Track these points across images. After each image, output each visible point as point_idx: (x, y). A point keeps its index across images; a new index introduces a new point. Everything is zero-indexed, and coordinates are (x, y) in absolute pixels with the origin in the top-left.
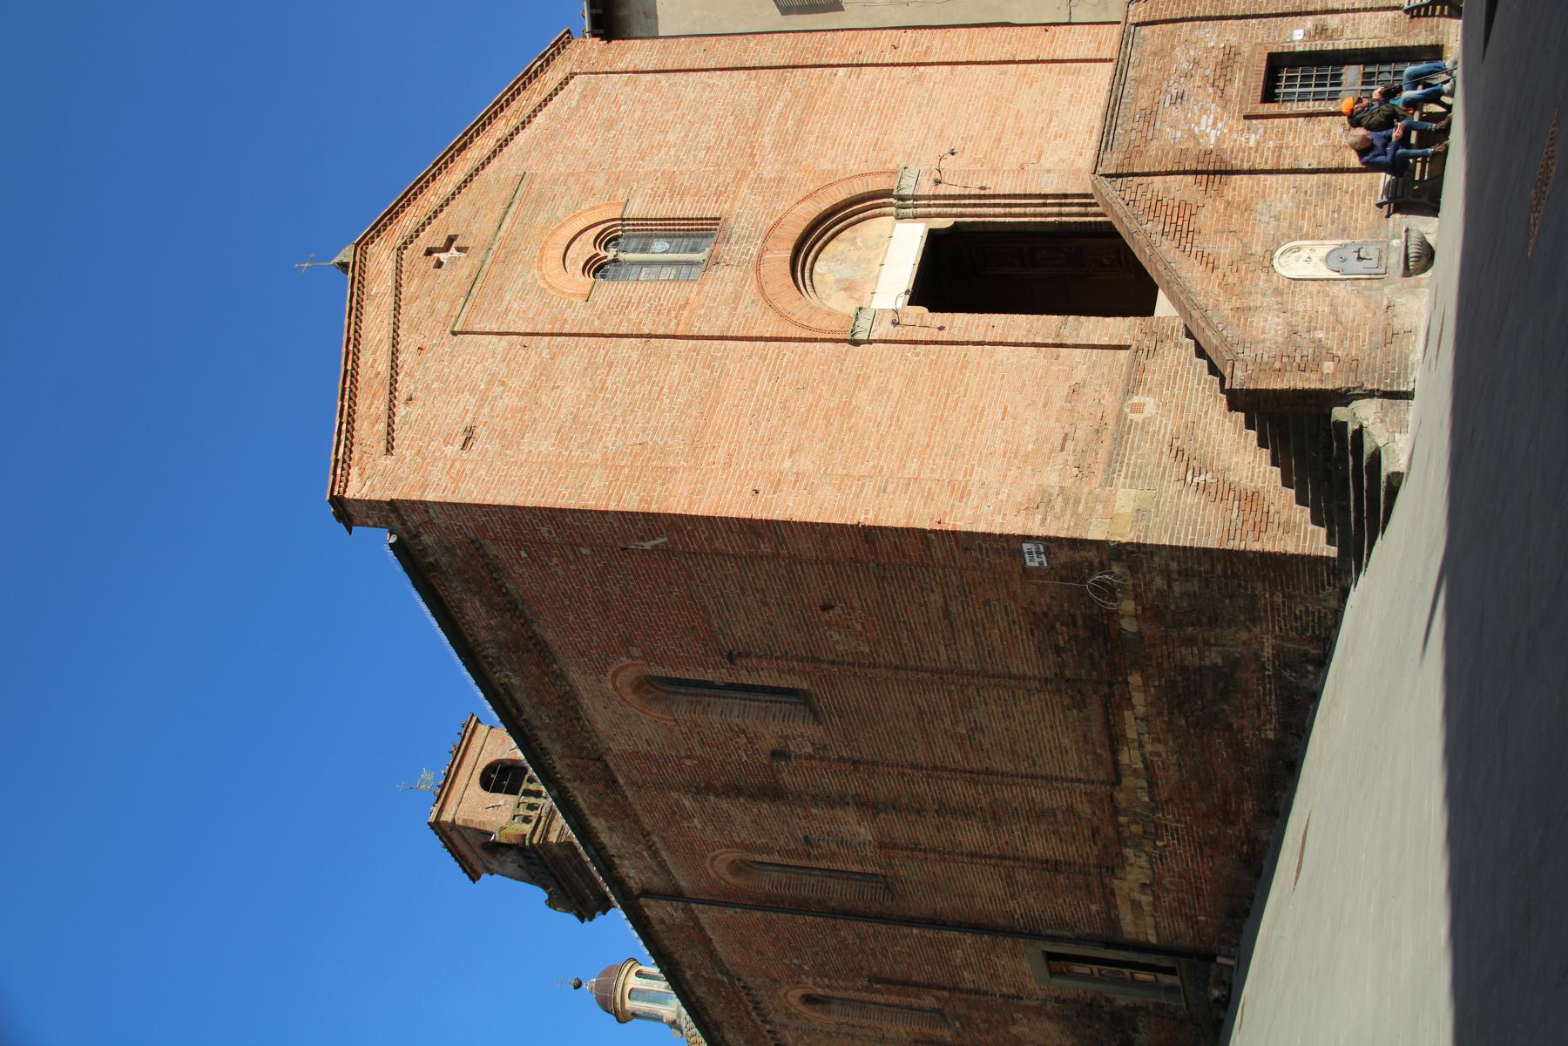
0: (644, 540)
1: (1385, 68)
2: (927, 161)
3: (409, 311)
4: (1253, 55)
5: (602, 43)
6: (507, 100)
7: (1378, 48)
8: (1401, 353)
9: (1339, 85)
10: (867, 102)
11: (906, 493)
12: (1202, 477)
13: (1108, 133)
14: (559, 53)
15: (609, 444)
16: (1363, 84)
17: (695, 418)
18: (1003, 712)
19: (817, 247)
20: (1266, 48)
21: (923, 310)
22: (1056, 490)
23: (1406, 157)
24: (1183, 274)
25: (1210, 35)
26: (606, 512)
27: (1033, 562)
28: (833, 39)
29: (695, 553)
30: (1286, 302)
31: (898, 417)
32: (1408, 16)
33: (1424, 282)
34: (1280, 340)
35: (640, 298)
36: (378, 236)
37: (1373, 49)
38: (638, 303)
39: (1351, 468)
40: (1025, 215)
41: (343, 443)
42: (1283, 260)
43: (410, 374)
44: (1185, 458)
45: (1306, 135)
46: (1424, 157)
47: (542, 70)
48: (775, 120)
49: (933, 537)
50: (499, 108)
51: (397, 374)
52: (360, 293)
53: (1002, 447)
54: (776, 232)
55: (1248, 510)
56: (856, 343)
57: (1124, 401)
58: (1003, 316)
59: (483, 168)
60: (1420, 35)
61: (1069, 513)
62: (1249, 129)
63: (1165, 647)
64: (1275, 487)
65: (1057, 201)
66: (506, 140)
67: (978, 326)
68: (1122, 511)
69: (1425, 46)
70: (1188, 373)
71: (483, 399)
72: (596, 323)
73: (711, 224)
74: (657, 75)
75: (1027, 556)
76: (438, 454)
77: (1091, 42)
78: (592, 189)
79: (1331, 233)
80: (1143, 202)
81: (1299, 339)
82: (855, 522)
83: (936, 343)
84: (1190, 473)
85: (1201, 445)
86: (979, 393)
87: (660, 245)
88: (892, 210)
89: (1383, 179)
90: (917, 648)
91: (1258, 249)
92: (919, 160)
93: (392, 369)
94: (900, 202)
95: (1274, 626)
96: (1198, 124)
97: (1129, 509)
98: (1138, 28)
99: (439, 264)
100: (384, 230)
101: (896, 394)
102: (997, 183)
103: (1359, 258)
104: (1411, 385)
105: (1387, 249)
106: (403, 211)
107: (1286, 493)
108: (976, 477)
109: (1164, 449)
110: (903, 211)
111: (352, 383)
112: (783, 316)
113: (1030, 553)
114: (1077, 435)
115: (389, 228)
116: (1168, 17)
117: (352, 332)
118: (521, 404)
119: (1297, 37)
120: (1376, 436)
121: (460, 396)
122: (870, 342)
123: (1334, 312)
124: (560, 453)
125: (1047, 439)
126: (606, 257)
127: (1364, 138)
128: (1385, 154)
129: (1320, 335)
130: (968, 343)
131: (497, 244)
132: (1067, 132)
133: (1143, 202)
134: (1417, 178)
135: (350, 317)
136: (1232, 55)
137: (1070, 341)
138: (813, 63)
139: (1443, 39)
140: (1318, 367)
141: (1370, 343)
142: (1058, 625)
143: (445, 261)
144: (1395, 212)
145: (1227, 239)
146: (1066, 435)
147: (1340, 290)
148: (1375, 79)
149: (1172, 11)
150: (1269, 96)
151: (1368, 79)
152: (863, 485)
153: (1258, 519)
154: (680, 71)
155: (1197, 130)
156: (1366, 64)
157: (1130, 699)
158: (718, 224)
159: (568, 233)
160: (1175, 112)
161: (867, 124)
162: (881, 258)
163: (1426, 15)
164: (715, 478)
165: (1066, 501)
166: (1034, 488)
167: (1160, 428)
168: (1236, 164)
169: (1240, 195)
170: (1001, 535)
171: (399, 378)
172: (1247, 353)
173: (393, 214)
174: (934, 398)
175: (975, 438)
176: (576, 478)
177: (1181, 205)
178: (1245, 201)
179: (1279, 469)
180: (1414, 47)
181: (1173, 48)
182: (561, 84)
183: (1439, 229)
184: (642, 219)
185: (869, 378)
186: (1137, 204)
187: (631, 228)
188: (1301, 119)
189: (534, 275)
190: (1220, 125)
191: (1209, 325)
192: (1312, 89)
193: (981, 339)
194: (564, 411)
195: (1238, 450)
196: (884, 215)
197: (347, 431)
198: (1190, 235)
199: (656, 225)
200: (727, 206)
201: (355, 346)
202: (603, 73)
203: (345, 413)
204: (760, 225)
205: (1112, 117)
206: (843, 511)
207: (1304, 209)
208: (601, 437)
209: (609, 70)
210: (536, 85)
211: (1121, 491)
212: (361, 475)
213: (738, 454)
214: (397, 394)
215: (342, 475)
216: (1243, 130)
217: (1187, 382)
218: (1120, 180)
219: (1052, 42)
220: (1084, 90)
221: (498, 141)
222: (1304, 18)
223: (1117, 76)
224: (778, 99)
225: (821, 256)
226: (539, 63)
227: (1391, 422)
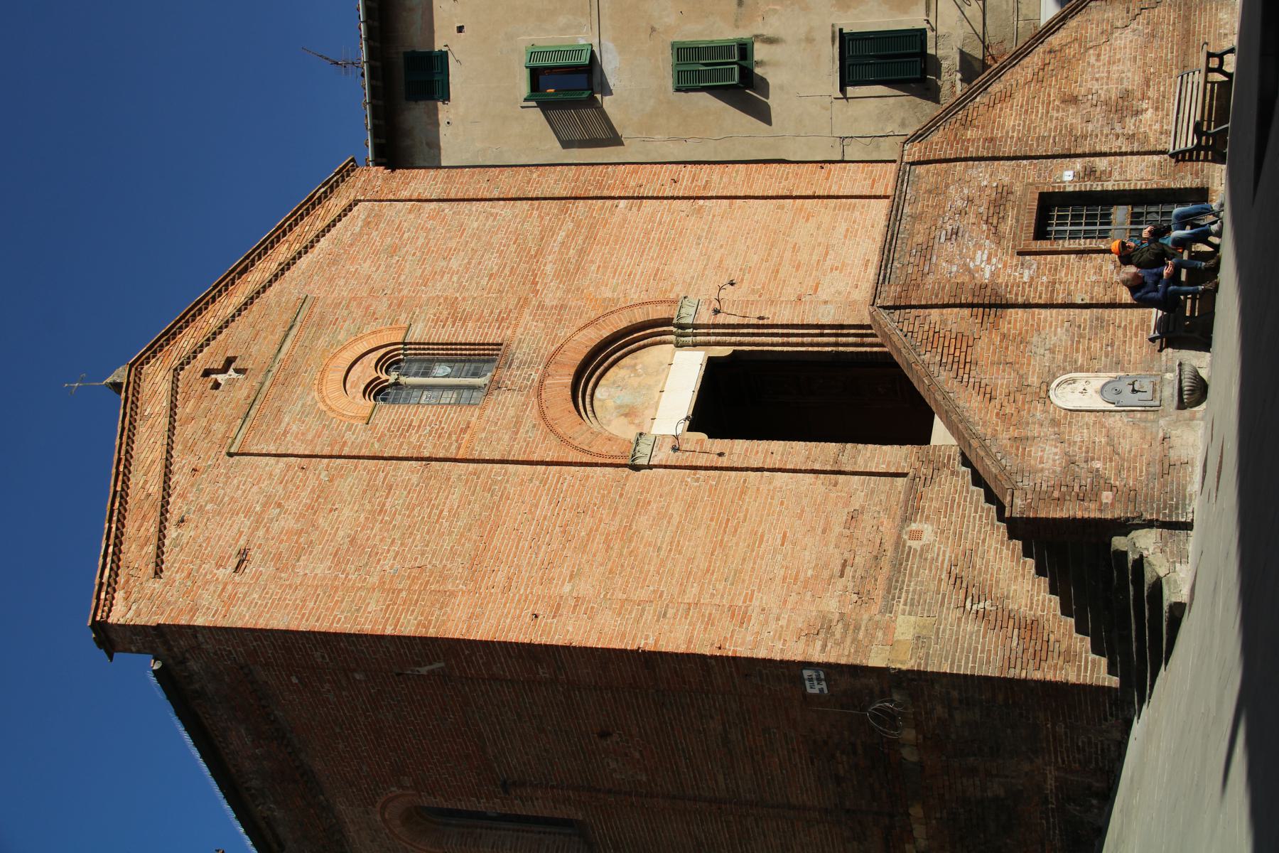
0: (420, 666)
1: (1153, 209)
2: (707, 290)
3: (185, 432)
4: (1024, 195)
5: (386, 171)
6: (290, 225)
7: (1146, 190)
8: (1178, 484)
9: (1109, 224)
10: (647, 233)
11: (686, 618)
12: (981, 605)
13: (886, 266)
14: (343, 180)
15: (387, 568)
16: (1132, 223)
17: (475, 541)
18: (781, 844)
19: (598, 373)
20: (1037, 188)
21: (703, 436)
22: (837, 616)
23: (1178, 293)
24: (961, 403)
25: (982, 175)
26: (382, 637)
27: (814, 689)
28: (614, 172)
29: (471, 679)
30: (1064, 433)
31: (679, 541)
32: (1174, 160)
33: (1198, 415)
34: (1058, 469)
35: (422, 421)
36: (154, 357)
37: (1140, 190)
38: (419, 426)
39: (1131, 598)
40: (803, 345)
41: (108, 566)
42: (1059, 391)
43: (182, 496)
44: (964, 585)
45: (1078, 271)
46: (1194, 293)
47: (326, 197)
48: (557, 249)
49: (713, 662)
50: (282, 233)
51: (169, 496)
52: (133, 414)
53: (782, 572)
54: (558, 358)
55: (1028, 639)
56: (637, 468)
57: (902, 528)
58: (782, 442)
59: (264, 292)
60: (1186, 179)
61: (849, 640)
62: (1022, 264)
63: (946, 778)
64: (1054, 615)
65: (834, 331)
66: (288, 264)
67: (757, 452)
68: (901, 638)
69: (1191, 189)
70: (965, 501)
71: (258, 522)
72: (376, 445)
73: (493, 350)
74: (441, 204)
75: (807, 683)
76: (209, 577)
77: (865, 179)
78: (374, 313)
79: (1105, 366)
80: (921, 333)
81: (1077, 469)
82: (635, 647)
83: (716, 468)
84: (969, 601)
85: (980, 573)
86: (758, 519)
87: (441, 369)
88: (672, 338)
89: (1154, 314)
90: (695, 777)
91: (1034, 380)
92: (699, 290)
93: (164, 490)
94: (680, 331)
95: (1056, 758)
96: (973, 259)
97: (909, 637)
98: (913, 167)
99: (217, 385)
100: (161, 351)
102: (775, 314)
103: (1134, 391)
104: (1190, 516)
105: (1161, 381)
106: (180, 333)
107: (1066, 622)
108: (756, 602)
109: (943, 577)
110: (683, 339)
111: (121, 504)
112: (564, 440)
113: (811, 680)
114: (856, 561)
115: (166, 349)
116: (942, 157)
117: (123, 452)
118: (299, 526)
119: (1067, 177)
120: (1158, 565)
121: (235, 518)
122: (650, 467)
123: (1110, 442)
124: (337, 576)
125: (826, 565)
126: (387, 380)
127: (1136, 275)
128: (1156, 290)
129: (1097, 465)
130: (747, 469)
131: (277, 366)
132: (843, 265)
133: (921, 333)
134: (1188, 314)
135: (121, 438)
136: (1005, 194)
137: (848, 469)
138: (595, 195)
139: (1208, 182)
140: (1096, 496)
141: (1148, 473)
142: (838, 754)
143: (223, 383)
144: (1167, 347)
145: (1004, 371)
146: (846, 561)
147: (1116, 422)
148: (1144, 219)
149: (945, 152)
150: (1041, 233)
151: (1136, 219)
152: (643, 610)
153: (1038, 648)
154: (464, 200)
155: (972, 265)
156: (1134, 205)
157: (911, 831)
158: (500, 350)
159: (350, 356)
160: (950, 247)
161: (648, 255)
162: (661, 384)
163: (1191, 160)
164: (494, 602)
165: (846, 627)
166: (814, 613)
167: (938, 555)
168: (1011, 297)
169: (1015, 328)
170: (782, 661)
171: (171, 500)
172: (1026, 482)
173: (171, 335)
174: (714, 523)
175: (754, 563)
176: (353, 601)
177: (960, 336)
178: (1020, 334)
179: (1058, 598)
180: (1180, 189)
181: (947, 186)
182: (345, 210)
183: (1212, 364)
184: (424, 344)
185: (649, 502)
186: (915, 335)
187: (413, 352)
188: (1073, 256)
189: (313, 397)
190: (994, 260)
191: (987, 454)
192: (1083, 228)
193: (760, 465)
194: (341, 533)
195: (1016, 577)
196: (664, 343)
197: (114, 553)
198: (968, 366)
199: (438, 349)
200: (509, 332)
201: (125, 467)
202: (387, 201)
203: (113, 535)
204: (542, 351)
205: (889, 251)
206: (624, 635)
207: (1078, 342)
208: (379, 560)
209: (393, 198)
210: (320, 211)
211: (900, 618)
212: (126, 599)
213: (518, 578)
214: (168, 515)
215: (106, 599)
216: (1016, 265)
217: (964, 510)
218: (898, 312)
219: (827, 179)
220: (859, 225)
221: (280, 264)
222: (1073, 160)
223: (894, 212)
224: (560, 229)
225: (602, 382)
226: (323, 190)
227: (1171, 552)
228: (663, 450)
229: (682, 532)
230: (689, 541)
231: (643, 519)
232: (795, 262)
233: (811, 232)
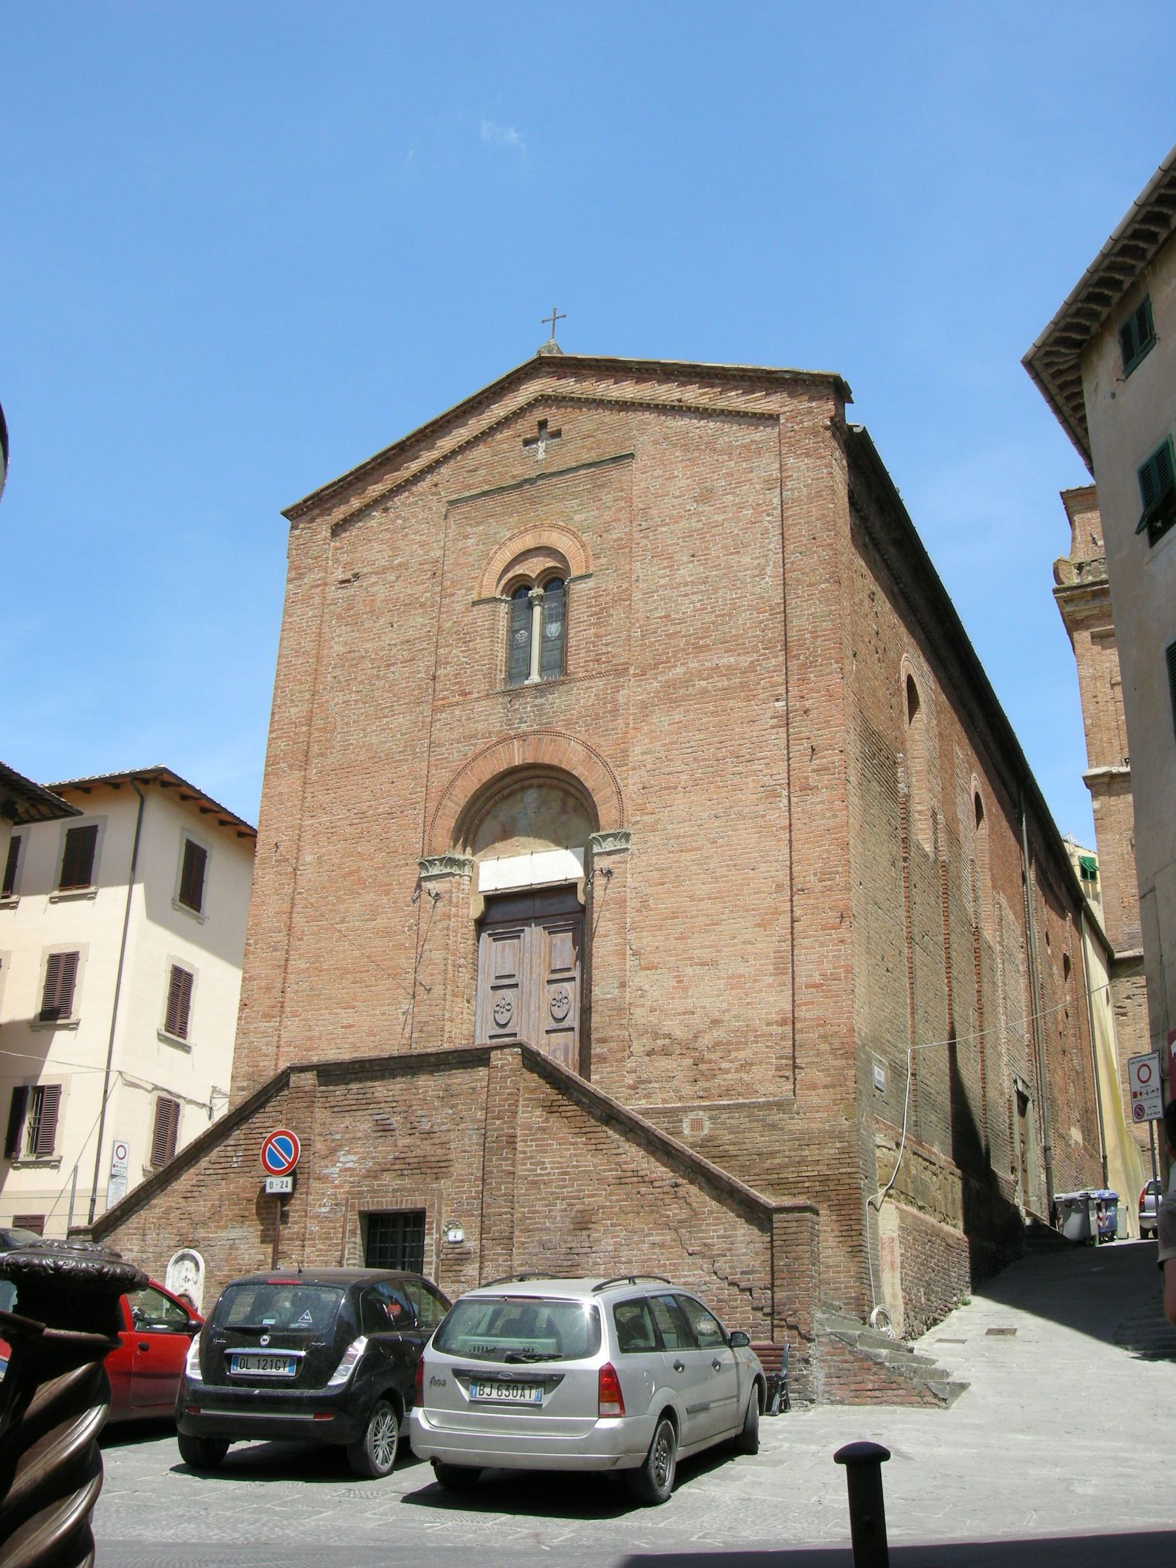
149: (499, 1094)
200: (581, 675)
231: (372, 896)
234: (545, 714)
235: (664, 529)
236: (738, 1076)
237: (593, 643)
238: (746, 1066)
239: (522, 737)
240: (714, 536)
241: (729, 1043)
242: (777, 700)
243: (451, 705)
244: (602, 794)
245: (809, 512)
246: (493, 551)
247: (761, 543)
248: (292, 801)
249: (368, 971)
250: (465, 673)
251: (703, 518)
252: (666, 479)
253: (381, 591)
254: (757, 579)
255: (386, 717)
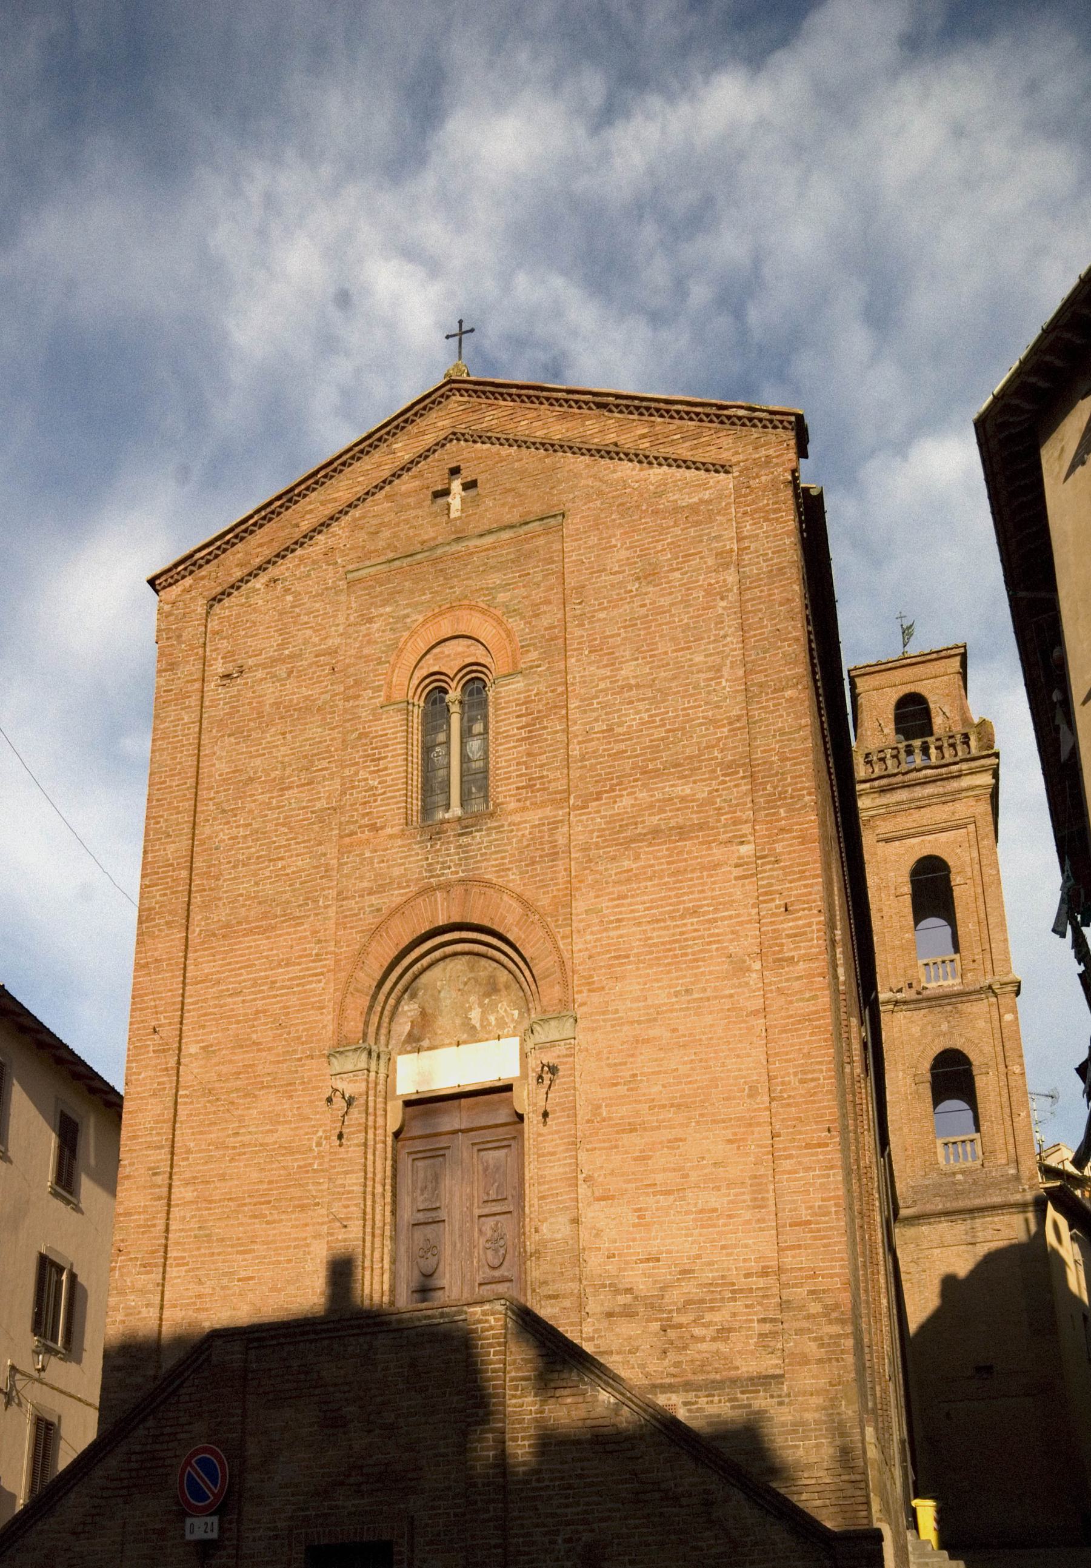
31: (244, 1153)
48: (658, 795)
101: (270, 1139)
159: (474, 624)
219: (808, 1146)
228: (351, 1085)
229: (256, 1152)
230: (246, 1166)
232: (651, 1150)
233: (707, 1156)
234: (471, 857)
235: (602, 615)
236: (714, 1346)
237: (525, 763)
238: (723, 1333)
239: (446, 887)
240: (660, 625)
241: (702, 1301)
242: (742, 843)
243: (360, 843)
244: (543, 963)
245: (770, 595)
246: (403, 640)
247: (715, 635)
248: (172, 971)
249: (269, 1202)
250: (375, 801)
251: (647, 601)
252: (603, 549)
253: (270, 692)
254: (713, 683)
255: (282, 859)
